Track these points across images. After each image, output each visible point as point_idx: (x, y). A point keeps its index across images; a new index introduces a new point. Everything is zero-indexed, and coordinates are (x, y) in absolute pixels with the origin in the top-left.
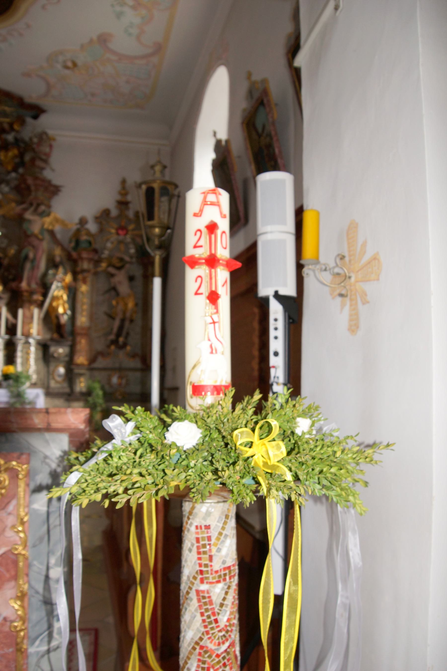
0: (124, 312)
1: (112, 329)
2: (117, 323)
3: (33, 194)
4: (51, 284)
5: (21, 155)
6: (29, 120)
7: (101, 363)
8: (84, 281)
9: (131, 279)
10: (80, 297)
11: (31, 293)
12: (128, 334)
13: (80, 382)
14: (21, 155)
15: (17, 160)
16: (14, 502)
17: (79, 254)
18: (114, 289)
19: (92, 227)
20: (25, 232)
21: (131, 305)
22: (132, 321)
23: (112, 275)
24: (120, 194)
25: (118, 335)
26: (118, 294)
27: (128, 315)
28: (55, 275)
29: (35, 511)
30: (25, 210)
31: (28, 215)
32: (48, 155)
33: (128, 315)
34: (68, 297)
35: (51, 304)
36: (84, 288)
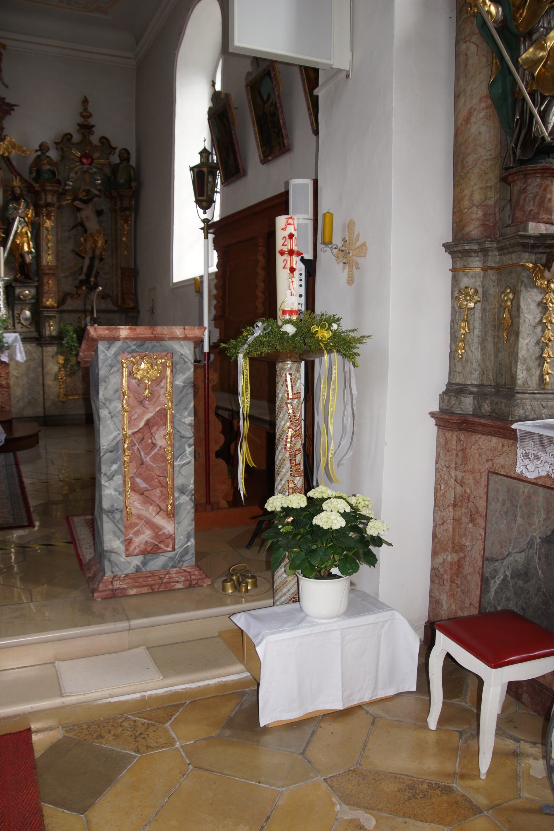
0: (94, 252)
1: (81, 268)
2: (87, 262)
4: (14, 220)
7: (70, 304)
9: (99, 213)
10: (44, 233)
12: (98, 273)
13: (50, 326)
16: (164, 381)
18: (82, 224)
19: (53, 154)
23: (79, 210)
24: (81, 115)
25: (88, 275)
26: (86, 231)
27: (98, 253)
28: (17, 209)
29: (177, 385)
35: (14, 241)
36: (48, 224)
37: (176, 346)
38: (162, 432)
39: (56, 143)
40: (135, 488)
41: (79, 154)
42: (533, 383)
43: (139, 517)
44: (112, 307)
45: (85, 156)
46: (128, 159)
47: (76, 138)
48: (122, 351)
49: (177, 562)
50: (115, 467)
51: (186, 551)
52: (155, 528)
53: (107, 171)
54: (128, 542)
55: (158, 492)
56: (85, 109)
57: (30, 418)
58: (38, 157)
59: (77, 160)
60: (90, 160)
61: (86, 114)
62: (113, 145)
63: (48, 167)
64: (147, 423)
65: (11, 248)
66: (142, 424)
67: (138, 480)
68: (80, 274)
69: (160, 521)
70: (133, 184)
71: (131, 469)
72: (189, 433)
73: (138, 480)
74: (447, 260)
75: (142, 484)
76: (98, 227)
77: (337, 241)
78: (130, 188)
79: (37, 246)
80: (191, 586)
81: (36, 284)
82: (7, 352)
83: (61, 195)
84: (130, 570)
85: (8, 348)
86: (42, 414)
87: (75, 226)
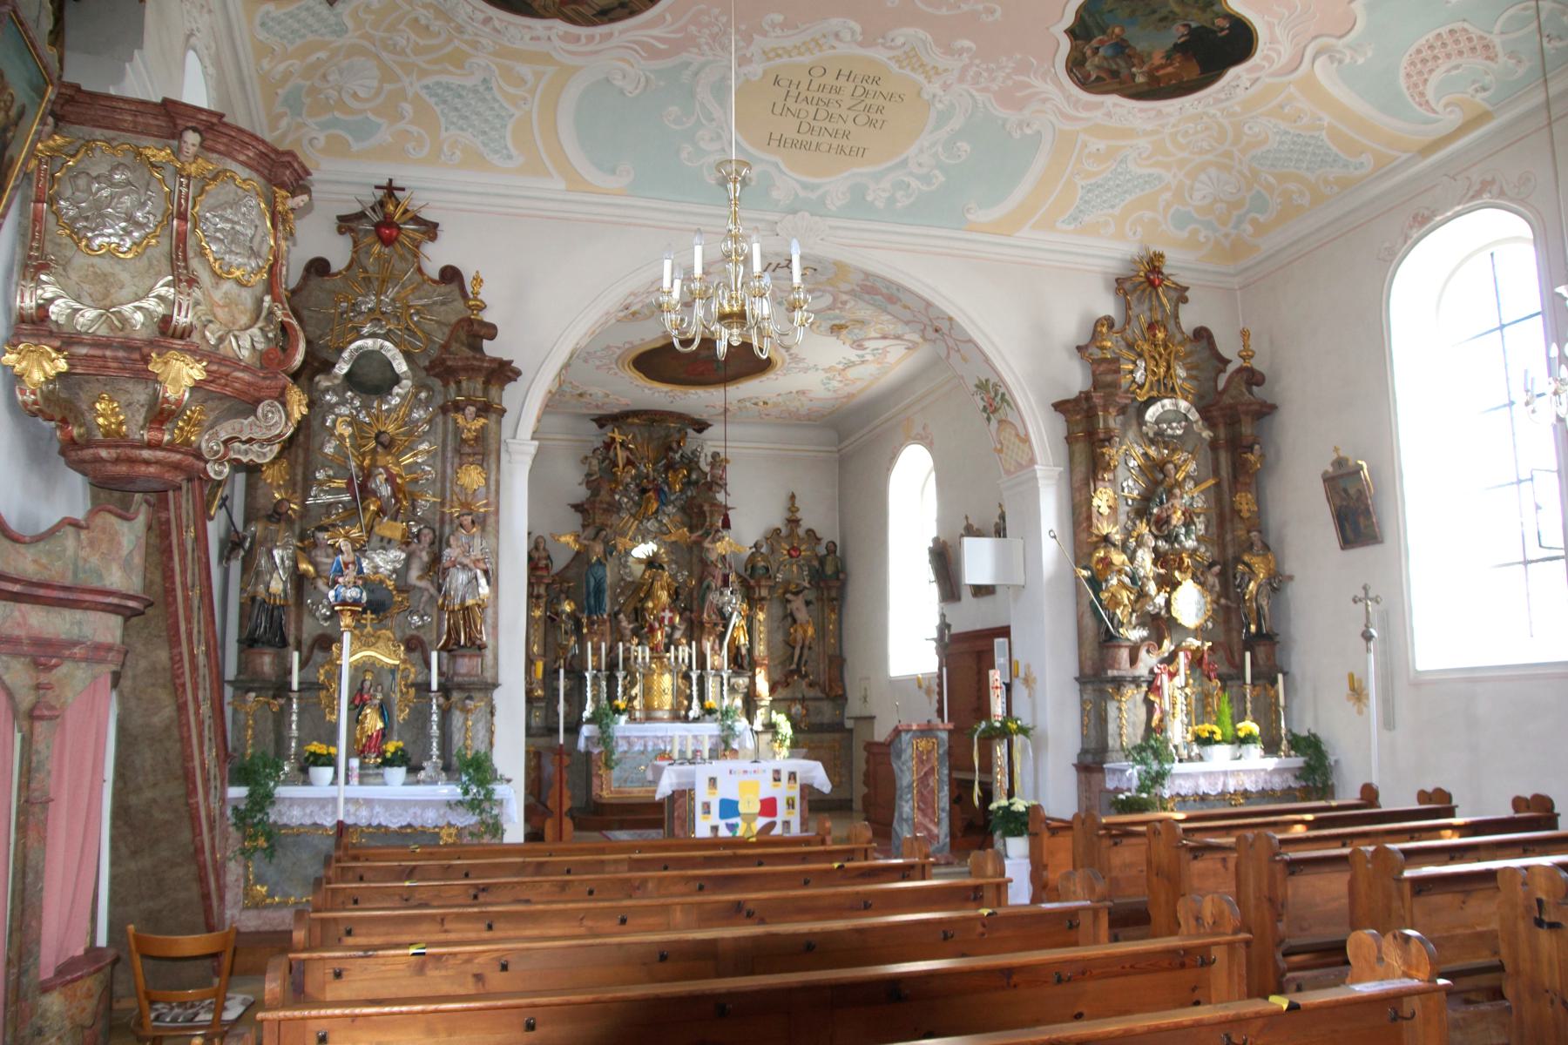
5: (689, 475)
6: (690, 432)
8: (761, 610)
9: (808, 603)
11: (716, 625)
15: (685, 480)
18: (791, 615)
21: (810, 631)
23: (788, 601)
24: (789, 509)
25: (798, 665)
26: (794, 621)
27: (807, 643)
31: (707, 544)
36: (761, 616)
42: (1117, 746)
44: (820, 695)
45: (793, 548)
47: (784, 532)
48: (913, 737)
52: (929, 830)
53: (816, 563)
55: (930, 811)
56: (793, 505)
61: (792, 509)
62: (819, 535)
63: (762, 564)
64: (926, 774)
70: (841, 576)
74: (1077, 686)
75: (922, 806)
76: (807, 617)
77: (1022, 674)
78: (838, 579)
79: (751, 641)
81: (750, 674)
82: (737, 740)
83: (771, 588)
87: (785, 617)
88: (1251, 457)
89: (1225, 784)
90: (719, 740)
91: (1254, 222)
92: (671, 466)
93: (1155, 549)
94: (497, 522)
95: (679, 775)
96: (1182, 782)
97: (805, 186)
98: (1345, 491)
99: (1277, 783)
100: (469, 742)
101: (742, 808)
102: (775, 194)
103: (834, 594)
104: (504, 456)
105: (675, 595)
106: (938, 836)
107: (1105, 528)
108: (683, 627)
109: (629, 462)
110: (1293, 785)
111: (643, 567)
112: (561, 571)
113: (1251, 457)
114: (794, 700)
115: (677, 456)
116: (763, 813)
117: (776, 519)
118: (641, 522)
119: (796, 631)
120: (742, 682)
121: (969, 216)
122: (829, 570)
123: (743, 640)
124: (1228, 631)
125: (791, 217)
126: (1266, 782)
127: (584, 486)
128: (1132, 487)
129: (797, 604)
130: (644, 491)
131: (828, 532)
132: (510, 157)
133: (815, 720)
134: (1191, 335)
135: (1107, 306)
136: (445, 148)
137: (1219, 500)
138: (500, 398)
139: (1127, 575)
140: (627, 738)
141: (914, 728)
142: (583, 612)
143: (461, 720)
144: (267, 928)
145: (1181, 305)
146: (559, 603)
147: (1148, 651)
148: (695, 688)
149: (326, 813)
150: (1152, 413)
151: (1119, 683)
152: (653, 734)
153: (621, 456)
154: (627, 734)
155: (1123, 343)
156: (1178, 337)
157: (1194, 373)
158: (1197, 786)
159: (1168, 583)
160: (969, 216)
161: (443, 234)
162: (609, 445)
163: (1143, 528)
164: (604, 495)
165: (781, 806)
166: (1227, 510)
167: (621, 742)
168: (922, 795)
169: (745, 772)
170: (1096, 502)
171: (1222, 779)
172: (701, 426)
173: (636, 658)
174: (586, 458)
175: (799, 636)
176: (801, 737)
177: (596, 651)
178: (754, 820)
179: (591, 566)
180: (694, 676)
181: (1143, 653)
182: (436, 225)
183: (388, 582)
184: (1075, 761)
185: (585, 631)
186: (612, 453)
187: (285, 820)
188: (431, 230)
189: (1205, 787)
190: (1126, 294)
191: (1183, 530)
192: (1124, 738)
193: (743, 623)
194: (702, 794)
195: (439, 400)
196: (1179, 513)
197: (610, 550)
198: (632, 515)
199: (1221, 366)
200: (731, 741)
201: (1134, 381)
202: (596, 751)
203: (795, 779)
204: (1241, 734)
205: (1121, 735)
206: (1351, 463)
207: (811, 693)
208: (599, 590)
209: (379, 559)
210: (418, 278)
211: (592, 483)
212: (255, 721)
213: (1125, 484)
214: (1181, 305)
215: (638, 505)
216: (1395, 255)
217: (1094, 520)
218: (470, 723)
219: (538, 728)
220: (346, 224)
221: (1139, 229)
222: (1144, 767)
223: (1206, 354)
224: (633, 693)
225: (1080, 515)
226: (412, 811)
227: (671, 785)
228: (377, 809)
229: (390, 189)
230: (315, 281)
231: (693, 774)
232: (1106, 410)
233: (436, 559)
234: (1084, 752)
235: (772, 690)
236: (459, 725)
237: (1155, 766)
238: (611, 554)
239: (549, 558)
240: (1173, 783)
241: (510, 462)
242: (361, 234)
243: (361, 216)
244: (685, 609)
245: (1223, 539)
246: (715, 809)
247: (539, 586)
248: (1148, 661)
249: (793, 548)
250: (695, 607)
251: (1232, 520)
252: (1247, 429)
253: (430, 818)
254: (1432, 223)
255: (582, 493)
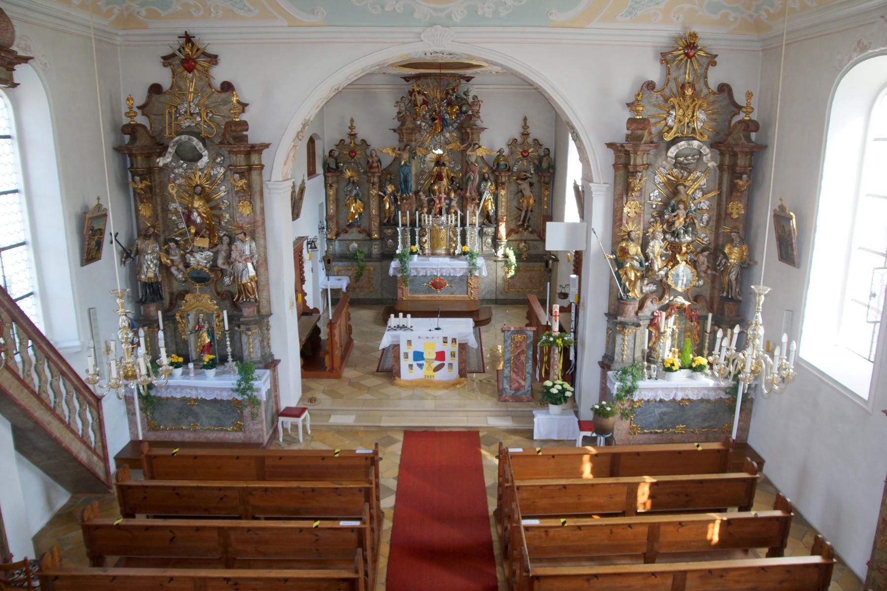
1: (520, 216)
2: (523, 214)
3: (470, 137)
4: (484, 192)
5: (460, 107)
6: (463, 81)
9: (531, 185)
10: (500, 197)
11: (473, 200)
12: (530, 218)
14: (460, 107)
17: (500, 174)
18: (521, 191)
19: (506, 151)
20: (466, 161)
21: (531, 201)
22: (532, 211)
23: (520, 184)
24: (523, 127)
25: (524, 221)
26: (523, 196)
27: (530, 209)
28: (485, 186)
30: (467, 148)
32: (478, 112)
33: (530, 209)
34: (493, 199)
36: (503, 192)
37: (528, 332)
38: (523, 356)
39: (509, 145)
40: (513, 371)
41: (521, 151)
42: (620, 360)
43: (515, 379)
46: (549, 155)
49: (525, 394)
50: (508, 365)
51: (528, 391)
54: (511, 386)
56: (525, 123)
57: (489, 300)
58: (498, 155)
59: (520, 153)
60: (527, 154)
63: (503, 162)
64: (519, 353)
65: (482, 208)
66: (517, 353)
67: (515, 369)
68: (519, 221)
69: (521, 381)
70: (551, 171)
71: (513, 366)
72: (531, 357)
73: (515, 369)
74: (606, 318)
75: (515, 370)
80: (528, 401)
81: (495, 226)
82: (478, 271)
84: (511, 394)
85: (479, 268)
86: (494, 298)
87: (518, 193)
88: (741, 183)
89: (675, 395)
90: (468, 271)
91: (767, 11)
92: (450, 104)
93: (664, 239)
94: (264, 230)
95: (393, 337)
96: (646, 393)
97: (435, 10)
98: (783, 227)
99: (712, 396)
100: (251, 349)
101: (425, 356)
102: (416, 16)
103: (547, 180)
104: (265, 191)
105: (452, 180)
106: (524, 386)
107: (630, 227)
108: (456, 199)
109: (425, 103)
110: (723, 397)
111: (433, 164)
112: (388, 167)
113: (741, 183)
114: (521, 241)
115: (453, 98)
116: (437, 359)
117: (515, 132)
118: (433, 137)
119: (523, 201)
120: (490, 230)
121: (551, 18)
122: (545, 165)
123: (491, 207)
124: (713, 288)
125: (429, 29)
126: (704, 394)
127: (396, 119)
128: (656, 196)
129: (525, 186)
130: (434, 119)
131: (547, 142)
132: (249, 11)
133: (533, 252)
134: (715, 90)
135: (654, 73)
136: (212, 10)
137: (719, 204)
138: (260, 161)
139: (637, 261)
140: (416, 269)
141: (512, 329)
142: (398, 193)
143: (246, 339)
144: (158, 439)
145: (710, 67)
146: (385, 186)
147: (652, 302)
148: (459, 237)
149: (177, 392)
150: (672, 152)
151: (624, 325)
152: (431, 267)
153: (420, 99)
154: (416, 267)
155: (661, 99)
156: (705, 91)
157: (714, 116)
158: (656, 396)
159: (672, 261)
160: (551, 18)
161: (222, 59)
162: (411, 93)
163: (659, 228)
164: (409, 124)
165: (448, 356)
166: (723, 212)
167: (412, 271)
168: (516, 364)
169: (427, 338)
170: (626, 210)
171: (674, 392)
172: (468, 79)
173: (425, 221)
174: (397, 102)
175: (525, 205)
176: (521, 264)
177: (404, 215)
178: (433, 362)
179: (402, 166)
180: (459, 230)
181: (648, 303)
182: (216, 57)
183: (206, 269)
184: (600, 359)
185: (399, 203)
186: (413, 98)
187: (159, 395)
188: (213, 59)
189: (661, 395)
190: (667, 63)
191: (682, 231)
192: (625, 357)
193: (491, 197)
194: (404, 348)
195: (227, 162)
196: (682, 219)
197: (413, 155)
198: (427, 133)
199: (736, 110)
200: (473, 272)
201: (666, 125)
202: (399, 275)
203: (455, 342)
204: (694, 365)
205: (623, 355)
206: (787, 211)
207: (532, 237)
208: (406, 181)
209: (198, 256)
210: (209, 90)
211: (401, 118)
212: (150, 339)
213: (652, 195)
214: (710, 67)
215: (431, 126)
216: (842, 67)
217: (624, 222)
218: (251, 340)
219: (377, 254)
220: (167, 60)
221: (681, 16)
222: (622, 384)
223: (726, 102)
224: (424, 240)
225: (617, 218)
226: (216, 392)
227: (388, 342)
228: (200, 391)
229: (188, 38)
230: (155, 97)
231: (398, 337)
232: (635, 153)
233: (229, 256)
234: (605, 357)
235: (508, 235)
236: (245, 341)
237: (629, 384)
238: (414, 158)
239: (379, 161)
240: (640, 393)
241: (269, 193)
242: (176, 66)
243: (173, 55)
244: (459, 188)
245: (718, 231)
246: (411, 356)
247: (374, 177)
248: (651, 307)
249: (525, 151)
250: (464, 188)
251: (725, 220)
252: (742, 161)
253: (225, 396)
254: (867, 53)
255: (396, 124)
